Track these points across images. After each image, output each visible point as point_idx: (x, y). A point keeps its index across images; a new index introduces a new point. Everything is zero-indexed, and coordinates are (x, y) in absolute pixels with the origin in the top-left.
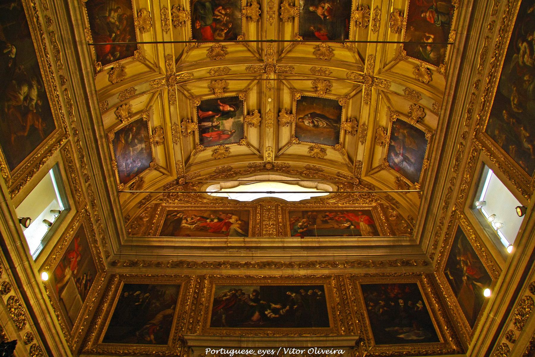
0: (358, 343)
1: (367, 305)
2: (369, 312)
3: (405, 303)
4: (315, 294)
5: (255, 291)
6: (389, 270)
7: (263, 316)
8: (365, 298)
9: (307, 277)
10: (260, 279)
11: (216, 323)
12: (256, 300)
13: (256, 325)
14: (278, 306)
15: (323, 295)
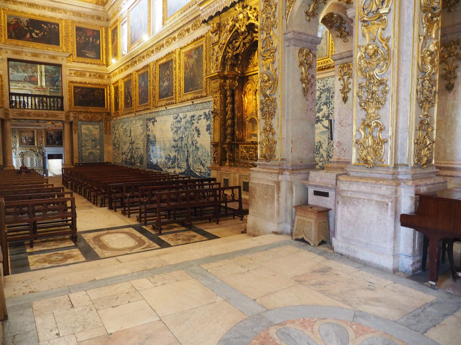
0: (70, 55)
1: (77, 38)
2: (77, 41)
3: (93, 40)
4: (55, 27)
5: (27, 21)
6: (90, 21)
7: (31, 36)
8: (76, 34)
9: (52, 18)
10: (29, 14)
11: (10, 37)
12: (27, 27)
13: (28, 40)
14: (38, 32)
15: (58, 29)
